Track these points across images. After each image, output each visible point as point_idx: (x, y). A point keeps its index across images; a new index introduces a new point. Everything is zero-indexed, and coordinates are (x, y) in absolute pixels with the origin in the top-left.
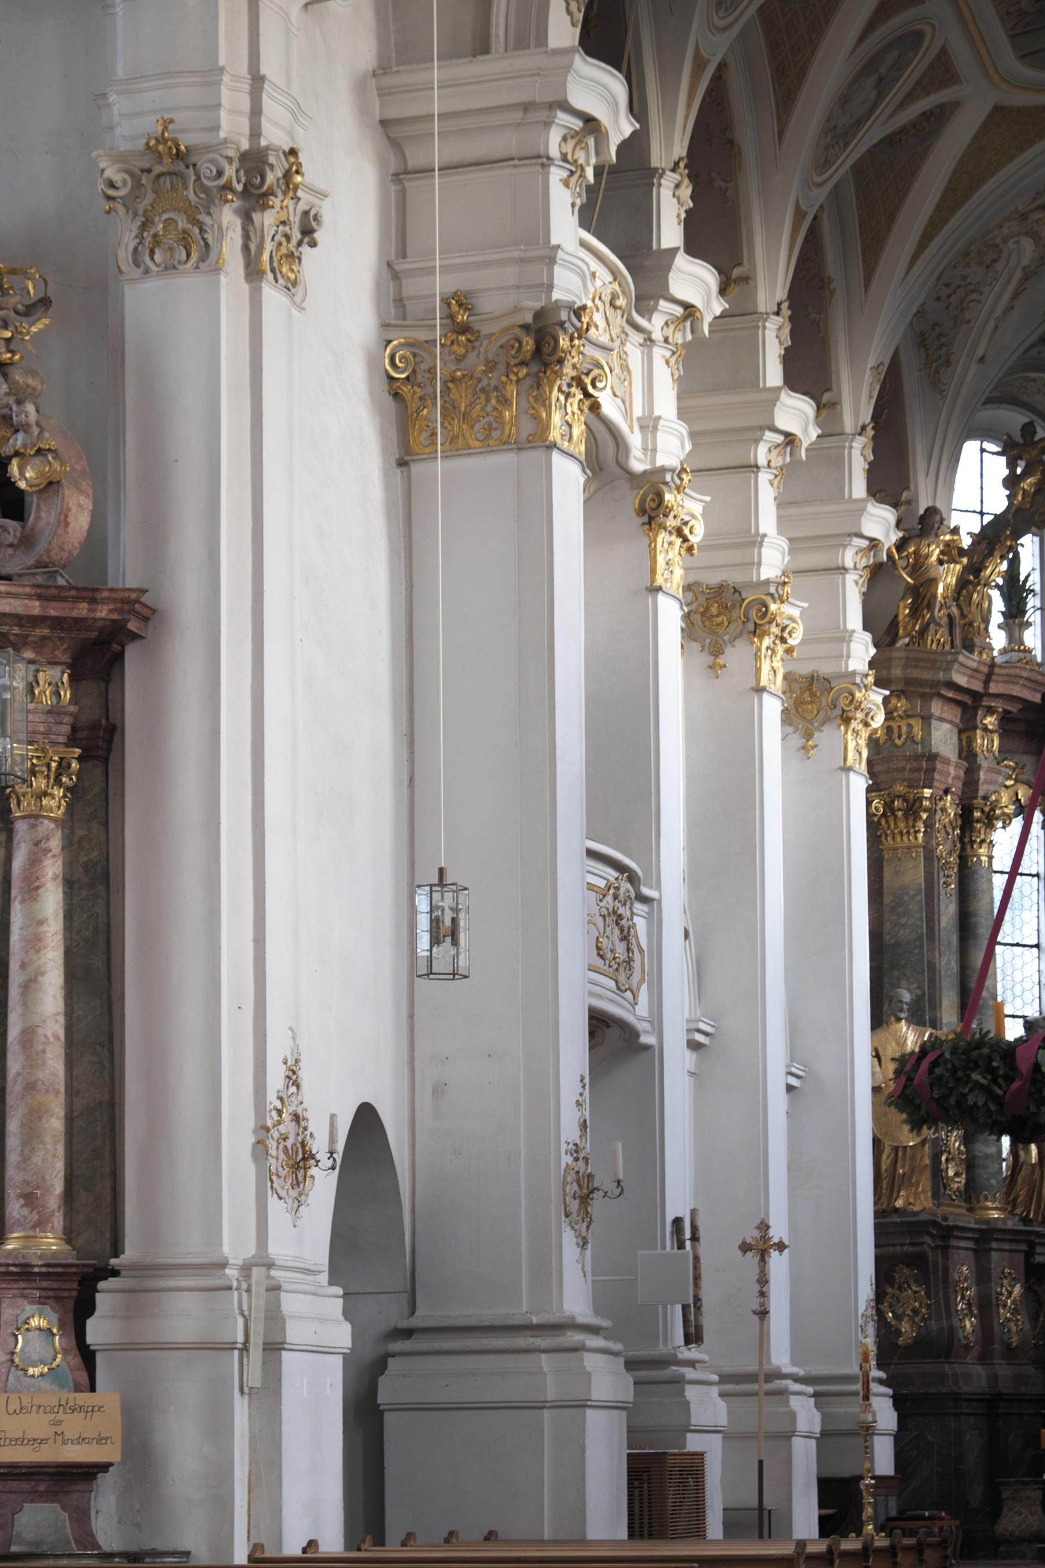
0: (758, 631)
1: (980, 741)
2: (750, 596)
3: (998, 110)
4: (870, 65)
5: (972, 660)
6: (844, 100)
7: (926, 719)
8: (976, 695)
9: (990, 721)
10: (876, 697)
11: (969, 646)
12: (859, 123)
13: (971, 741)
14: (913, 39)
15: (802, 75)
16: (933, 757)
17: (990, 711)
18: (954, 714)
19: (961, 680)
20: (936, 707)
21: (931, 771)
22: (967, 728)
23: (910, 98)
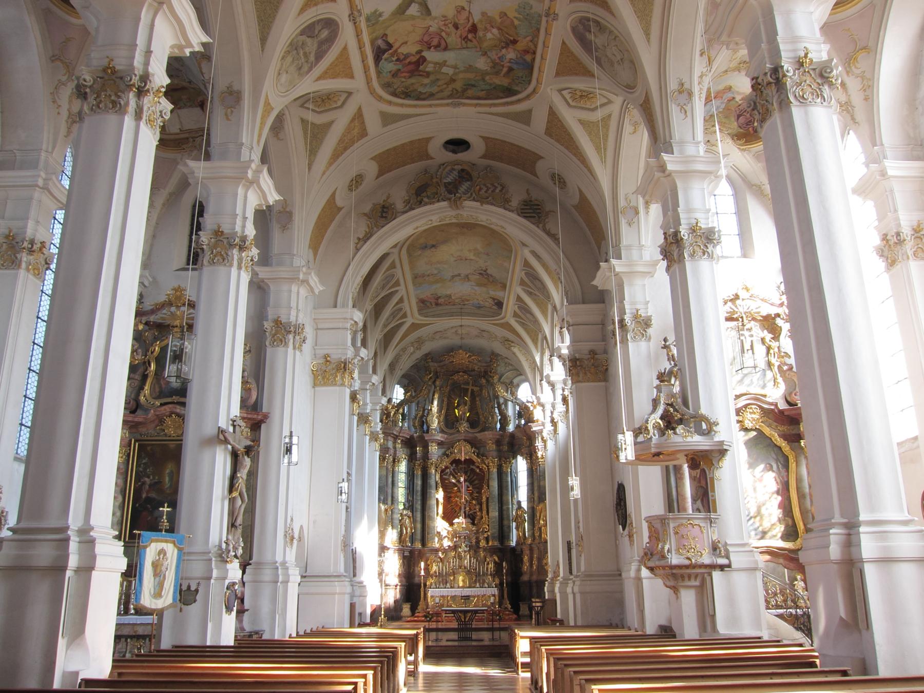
0: (366, 423)
1: (397, 446)
2: (364, 415)
3: (413, 323)
4: (392, 314)
5: (397, 429)
6: (387, 319)
7: (387, 440)
8: (397, 436)
9: (399, 441)
10: (381, 436)
11: (396, 426)
12: (389, 324)
13: (395, 445)
14: (401, 309)
15: (380, 314)
16: (388, 448)
17: (399, 439)
18: (392, 439)
19: (395, 433)
20: (389, 438)
21: (388, 451)
22: (395, 443)
23: (398, 320)
